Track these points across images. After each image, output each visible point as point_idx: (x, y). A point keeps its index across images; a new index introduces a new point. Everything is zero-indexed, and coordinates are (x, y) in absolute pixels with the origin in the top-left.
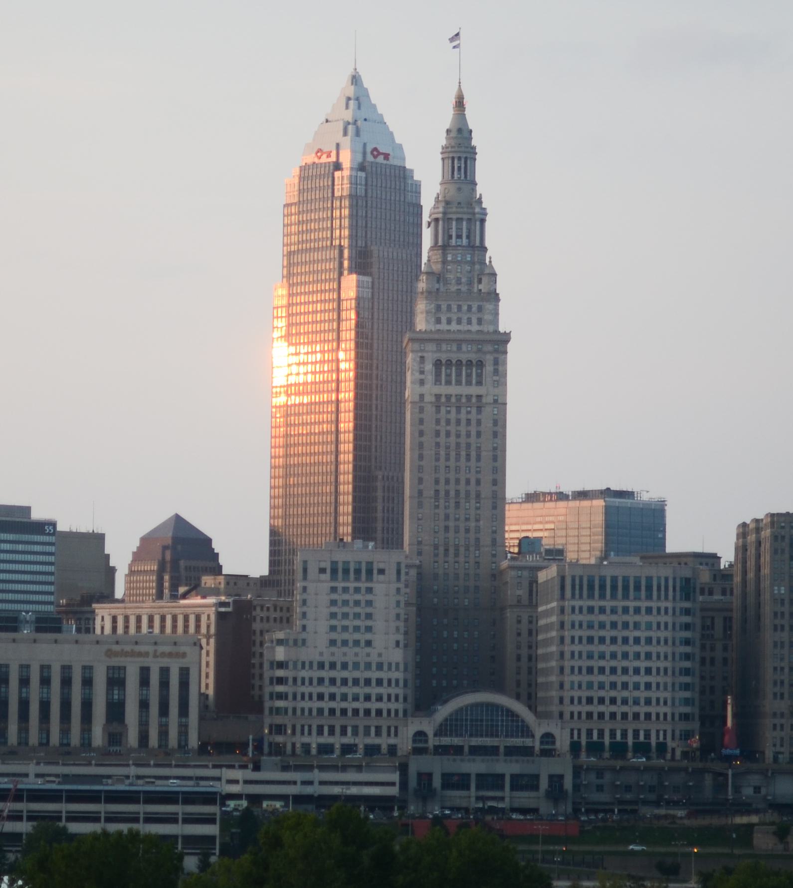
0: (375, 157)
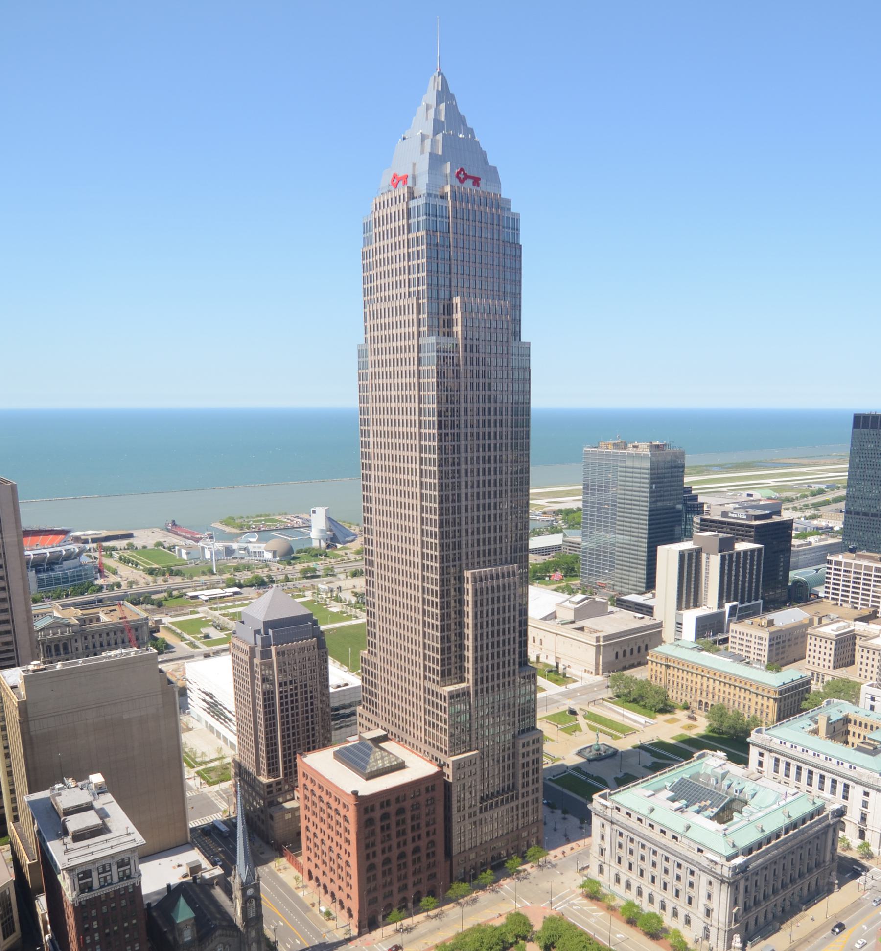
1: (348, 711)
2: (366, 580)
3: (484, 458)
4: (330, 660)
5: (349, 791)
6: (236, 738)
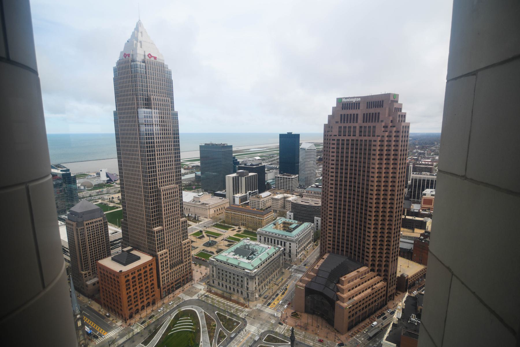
0: (150, 58)
1: (117, 242)
2: (121, 194)
3: (163, 149)
4: (108, 223)
5: (118, 271)
6: (70, 258)
